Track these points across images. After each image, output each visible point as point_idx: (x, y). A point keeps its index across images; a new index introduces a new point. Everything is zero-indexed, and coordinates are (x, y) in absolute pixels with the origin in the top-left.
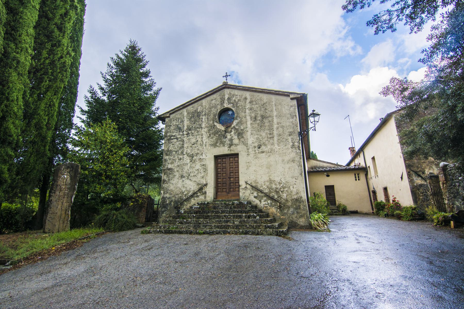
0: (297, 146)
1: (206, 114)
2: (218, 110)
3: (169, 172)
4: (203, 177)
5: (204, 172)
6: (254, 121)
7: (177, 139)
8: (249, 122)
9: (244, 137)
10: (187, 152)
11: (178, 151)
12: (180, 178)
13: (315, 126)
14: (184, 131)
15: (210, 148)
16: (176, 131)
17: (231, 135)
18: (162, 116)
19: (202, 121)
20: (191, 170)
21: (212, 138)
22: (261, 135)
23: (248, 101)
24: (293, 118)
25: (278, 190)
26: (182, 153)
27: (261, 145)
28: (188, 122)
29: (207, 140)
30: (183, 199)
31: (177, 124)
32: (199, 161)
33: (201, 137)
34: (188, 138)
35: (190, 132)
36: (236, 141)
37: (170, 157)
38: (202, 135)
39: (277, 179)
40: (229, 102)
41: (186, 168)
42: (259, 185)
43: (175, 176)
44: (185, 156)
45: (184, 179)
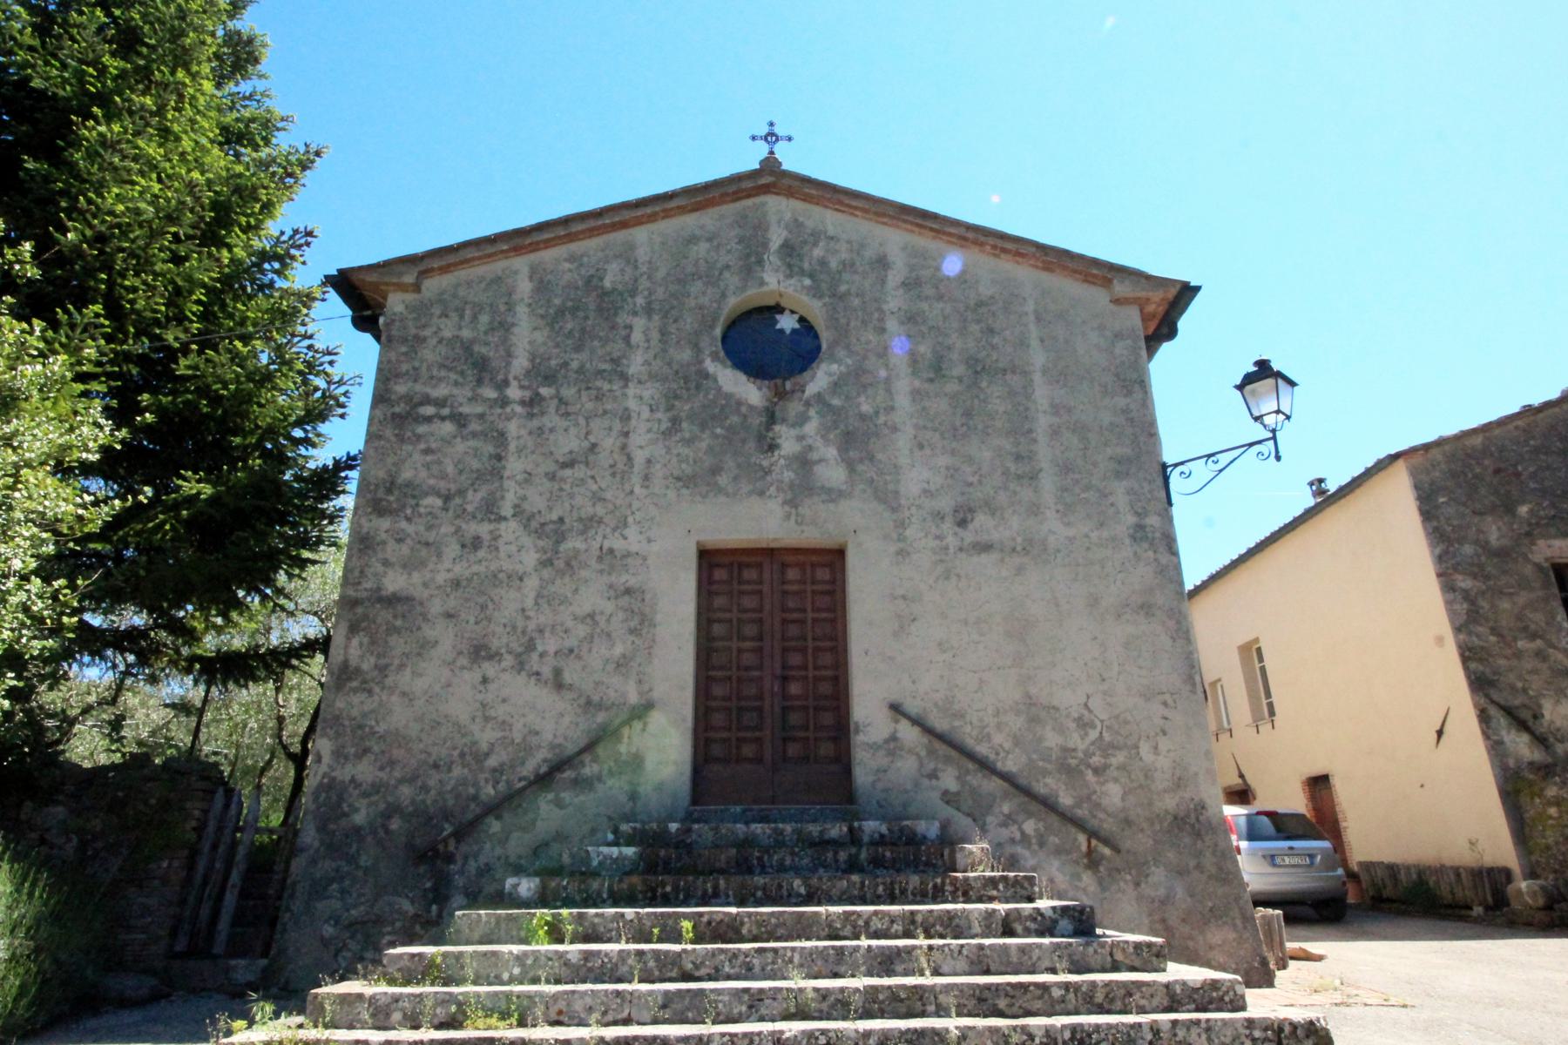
0: (1158, 535)
1: (656, 306)
2: (724, 295)
4: (622, 665)
5: (632, 631)
6: (931, 380)
7: (460, 420)
8: (903, 385)
9: (880, 456)
10: (526, 506)
11: (461, 493)
12: (463, 661)
13: (1274, 438)
14: (506, 383)
15: (671, 494)
16: (453, 376)
17: (801, 438)
18: (372, 278)
19: (627, 339)
20: (544, 617)
21: (688, 442)
22: (970, 460)
23: (894, 278)
24: (1129, 393)
25: (1073, 762)
26: (490, 510)
27: (971, 510)
28: (539, 337)
29: (659, 451)
30: (475, 798)
31: (466, 333)
33: (617, 426)
34: (535, 423)
35: (544, 391)
36: (832, 473)
37: (404, 524)
38: (626, 417)
39: (1069, 700)
40: (790, 266)
41: (510, 603)
43: (426, 645)
44: (510, 530)
45: (489, 668)
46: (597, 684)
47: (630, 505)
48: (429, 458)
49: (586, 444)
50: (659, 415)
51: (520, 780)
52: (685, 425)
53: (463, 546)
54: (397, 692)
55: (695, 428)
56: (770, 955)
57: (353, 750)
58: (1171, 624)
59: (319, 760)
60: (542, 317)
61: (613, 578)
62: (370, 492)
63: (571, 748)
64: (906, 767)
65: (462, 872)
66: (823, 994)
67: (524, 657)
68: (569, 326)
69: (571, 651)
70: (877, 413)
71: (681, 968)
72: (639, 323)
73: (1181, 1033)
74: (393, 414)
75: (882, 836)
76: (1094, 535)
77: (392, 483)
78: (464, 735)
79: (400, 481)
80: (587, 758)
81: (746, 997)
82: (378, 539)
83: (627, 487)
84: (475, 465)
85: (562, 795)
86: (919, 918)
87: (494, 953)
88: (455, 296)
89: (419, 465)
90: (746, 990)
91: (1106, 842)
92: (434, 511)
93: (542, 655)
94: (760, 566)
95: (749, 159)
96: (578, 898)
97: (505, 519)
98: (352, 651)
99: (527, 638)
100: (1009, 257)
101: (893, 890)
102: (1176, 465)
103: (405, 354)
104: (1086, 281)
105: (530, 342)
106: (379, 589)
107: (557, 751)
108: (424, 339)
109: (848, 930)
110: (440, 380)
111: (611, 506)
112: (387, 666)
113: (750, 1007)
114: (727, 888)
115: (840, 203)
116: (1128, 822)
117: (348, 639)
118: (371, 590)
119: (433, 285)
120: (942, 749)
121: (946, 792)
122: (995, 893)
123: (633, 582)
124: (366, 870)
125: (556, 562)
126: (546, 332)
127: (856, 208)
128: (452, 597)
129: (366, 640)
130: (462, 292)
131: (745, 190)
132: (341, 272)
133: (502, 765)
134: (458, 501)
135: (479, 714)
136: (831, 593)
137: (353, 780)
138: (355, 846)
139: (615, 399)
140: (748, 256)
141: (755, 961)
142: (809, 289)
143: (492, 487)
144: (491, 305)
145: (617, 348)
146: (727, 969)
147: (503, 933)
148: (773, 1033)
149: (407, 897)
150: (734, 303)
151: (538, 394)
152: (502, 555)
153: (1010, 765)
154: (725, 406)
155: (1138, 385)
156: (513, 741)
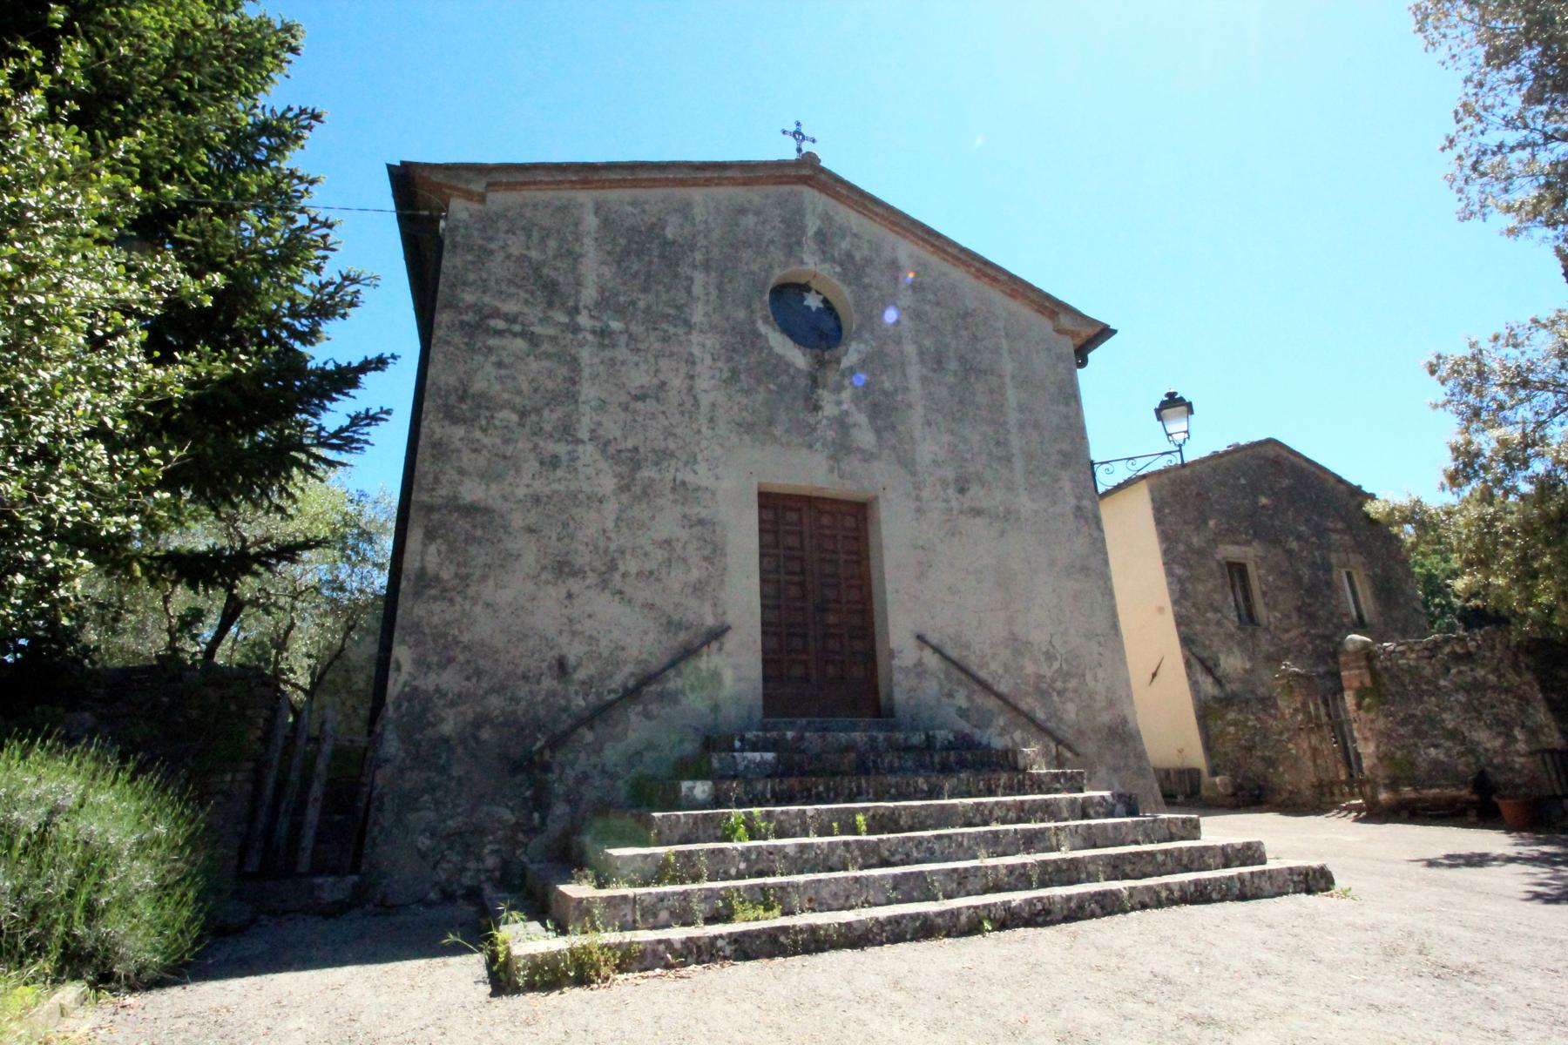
3: (463, 525)
4: (698, 589)
5: (706, 559)
7: (533, 340)
8: (914, 371)
10: (601, 432)
11: (538, 411)
13: (1180, 451)
14: (576, 310)
15: (735, 439)
16: (523, 295)
17: (839, 403)
18: (438, 178)
19: (688, 290)
21: (747, 392)
22: (965, 440)
25: (1044, 686)
26: (566, 430)
27: (967, 481)
29: (720, 397)
30: (566, 709)
32: (671, 497)
33: (684, 369)
34: (608, 354)
36: (864, 437)
37: (478, 434)
39: (1038, 637)
40: (823, 252)
41: (592, 524)
42: (973, 657)
43: (510, 558)
44: (587, 452)
45: (574, 585)
46: (677, 605)
47: (698, 444)
48: (503, 372)
49: (655, 381)
50: (719, 364)
51: (610, 692)
52: (743, 377)
53: (542, 463)
54: (480, 603)
55: (752, 381)
56: (946, 841)
57: (435, 659)
58: (1101, 583)
59: (399, 669)
60: (609, 253)
61: (686, 510)
62: (441, 397)
63: (655, 665)
64: (931, 688)
65: (560, 780)
66: (1011, 869)
67: (606, 576)
68: (635, 267)
69: (651, 573)
70: (896, 391)
71: (879, 855)
72: (699, 277)
73: (1256, 881)
74: (462, 322)
75: (950, 742)
76: (1051, 510)
77: (465, 391)
78: (552, 648)
79: (471, 391)
80: (671, 673)
81: (955, 876)
82: (452, 447)
83: (695, 426)
84: (550, 385)
85: (650, 707)
86: (1026, 807)
87: (721, 851)
88: (522, 215)
89: (492, 378)
90: (955, 870)
91: (1070, 748)
92: (511, 425)
93: (624, 575)
94: (799, 510)
95: (787, 151)
96: (745, 798)
97: (583, 442)
98: (428, 558)
99: (609, 558)
100: (986, 280)
101: (990, 785)
102: (1102, 463)
103: (472, 263)
104: (1038, 311)
105: (598, 276)
106: (456, 498)
107: (642, 666)
108: (492, 252)
109: (978, 819)
110: (511, 296)
111: (681, 443)
112: (468, 576)
113: (959, 884)
114: (868, 787)
115: (865, 207)
116: (1081, 733)
117: (425, 545)
118: (447, 496)
119: (499, 200)
120: (956, 674)
121: (960, 709)
122: (1058, 786)
123: (704, 514)
124: (459, 781)
125: (633, 489)
126: (614, 268)
127: (877, 214)
128: (533, 512)
129: (444, 548)
130: (528, 213)
131: (789, 176)
132: (405, 164)
133: (591, 678)
134: (534, 418)
135: (566, 628)
136: (856, 539)
137: (438, 690)
138: (444, 756)
139: (680, 343)
140: (789, 236)
141: (936, 847)
142: (839, 274)
143: (567, 409)
144: (558, 231)
145: (681, 297)
146: (915, 854)
147: (700, 832)
148: (1004, 903)
149: (507, 806)
150: (777, 275)
151: (608, 326)
152: (581, 477)
153: (1003, 687)
154: (779, 365)
155: (1070, 396)
156: (600, 654)
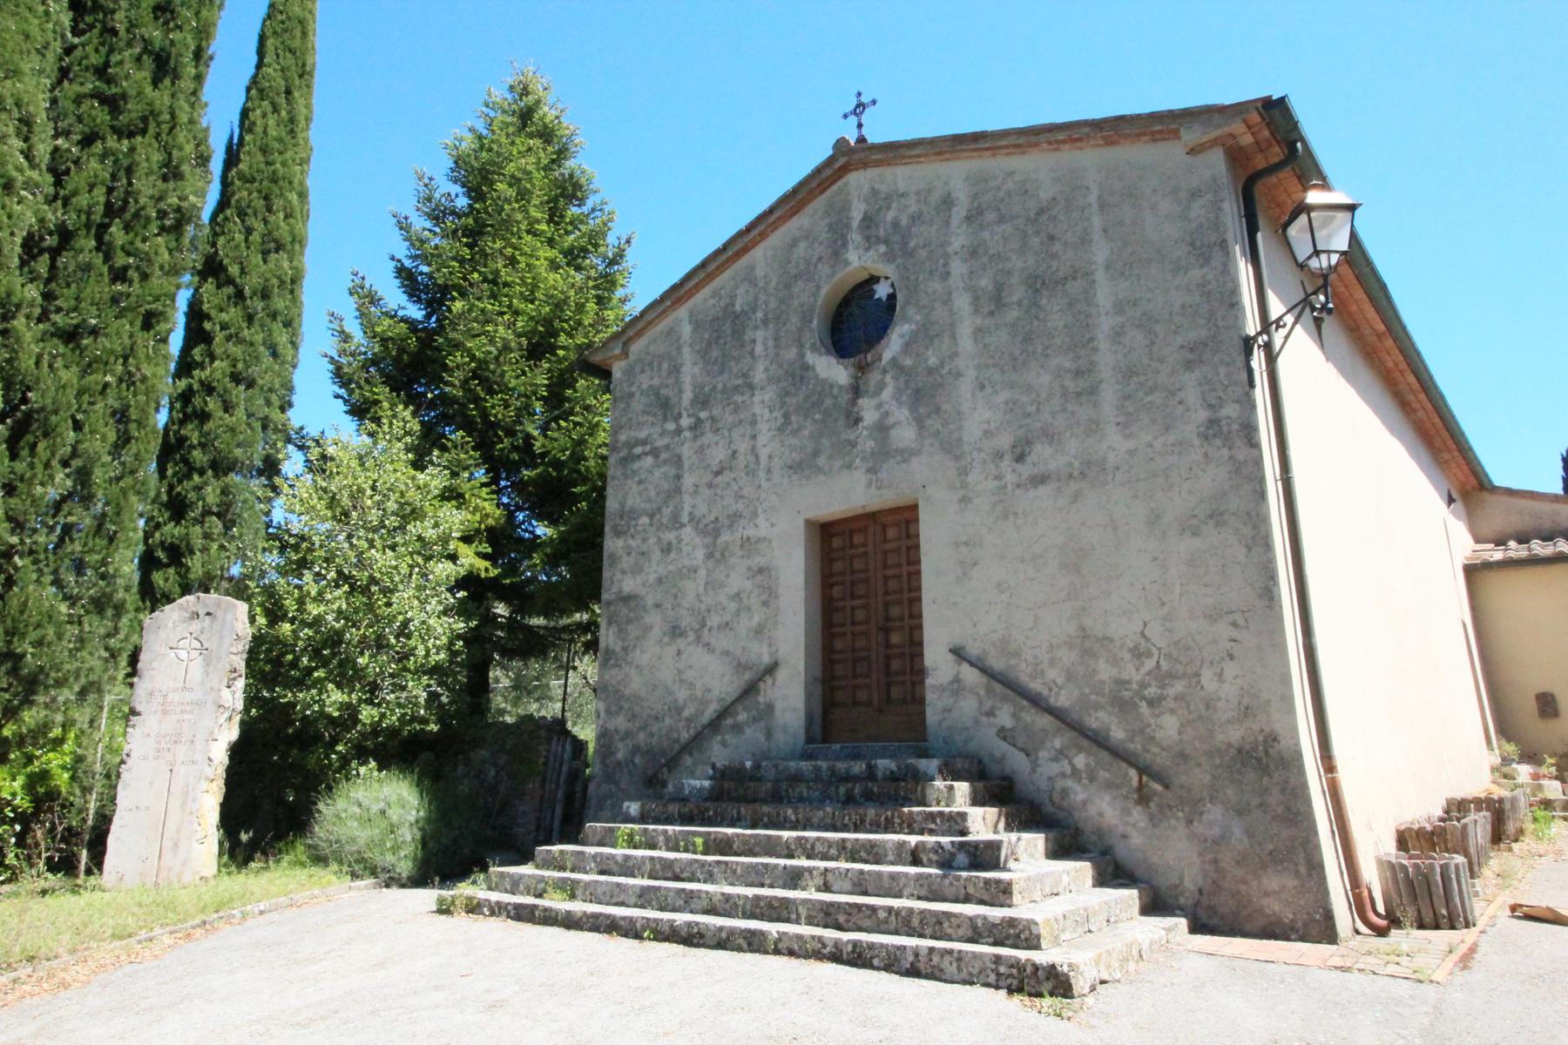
0: (1235, 427)
1: (770, 316)
2: (818, 287)
3: (624, 611)
4: (759, 631)
6: (992, 313)
7: (655, 452)
9: (945, 407)
11: (659, 509)
12: (666, 639)
14: (680, 415)
16: (650, 418)
19: (752, 353)
20: (708, 600)
21: (795, 433)
22: (1029, 388)
23: (958, 213)
24: (1207, 261)
25: (1127, 694)
26: (676, 522)
28: (696, 369)
31: (656, 382)
32: (740, 553)
34: (699, 443)
35: (703, 415)
36: (905, 435)
38: (754, 423)
39: (1124, 630)
40: (868, 238)
41: (692, 589)
42: (1023, 666)
43: (647, 629)
45: (681, 643)
49: (730, 452)
50: (776, 414)
52: (793, 418)
58: (1247, 531)
68: (715, 354)
69: (727, 624)
70: (942, 363)
73: (936, 959)
75: (892, 772)
79: (626, 509)
86: (849, 845)
90: (683, 890)
93: (710, 630)
100: (1067, 146)
104: (1155, 140)
116: (1183, 756)
120: (998, 687)
122: (933, 826)
131: (827, 179)
134: (658, 517)
148: (669, 921)
151: (699, 419)
152: (684, 554)
153: (1062, 700)
